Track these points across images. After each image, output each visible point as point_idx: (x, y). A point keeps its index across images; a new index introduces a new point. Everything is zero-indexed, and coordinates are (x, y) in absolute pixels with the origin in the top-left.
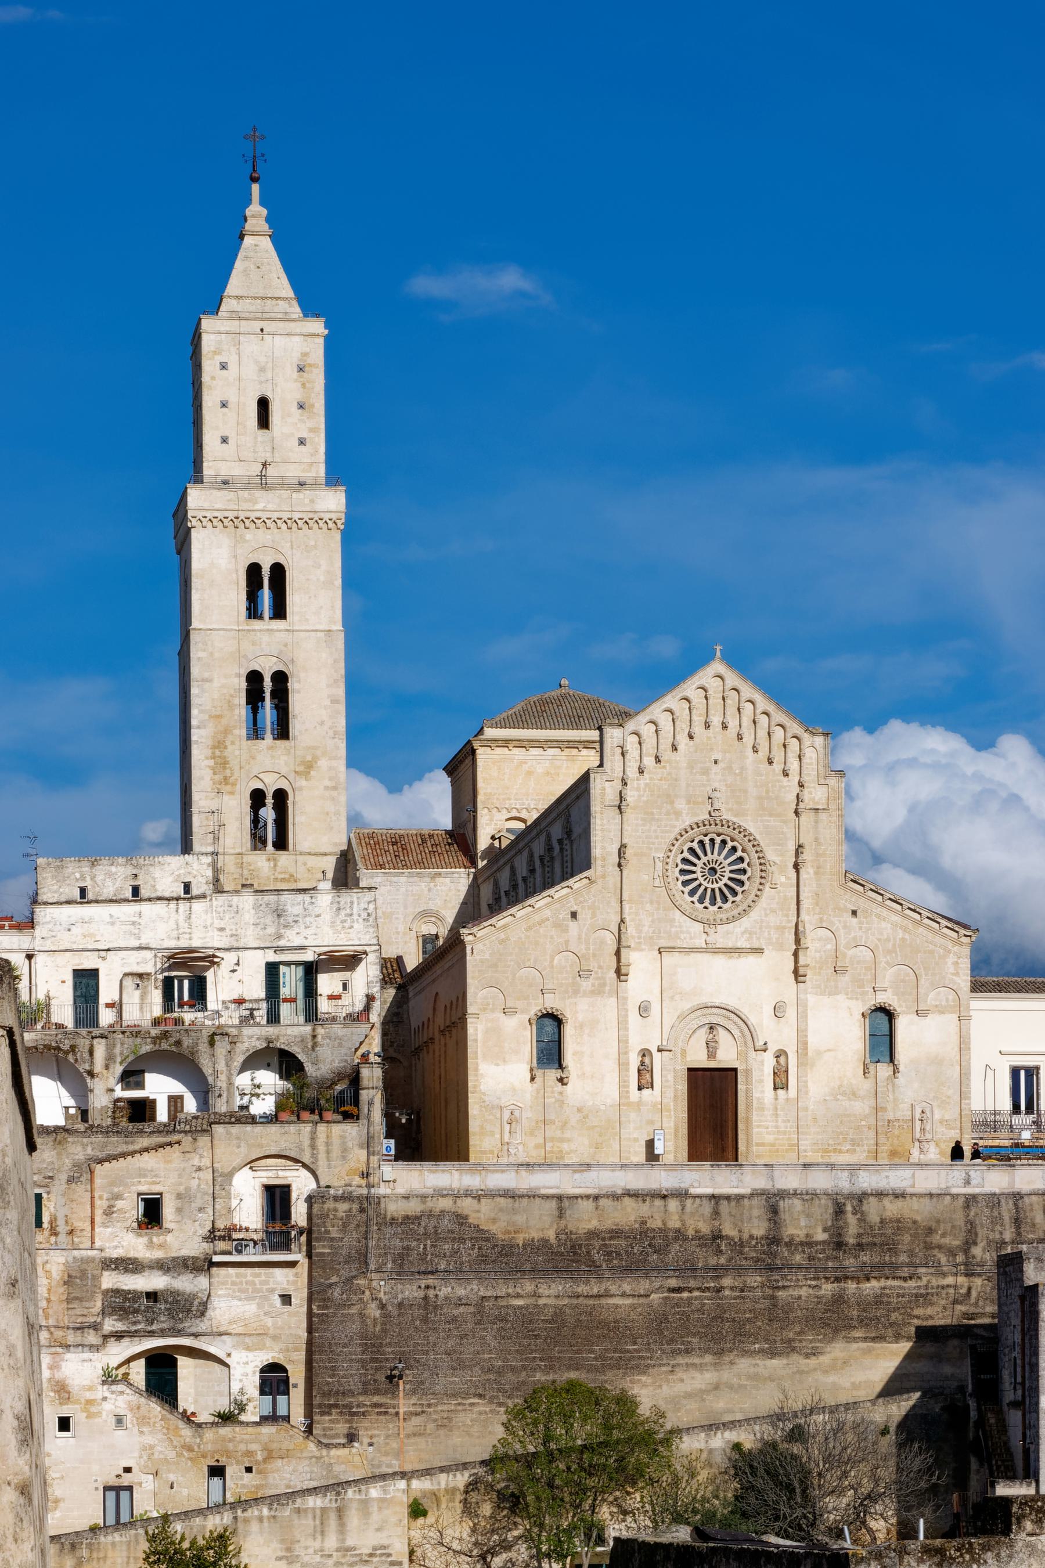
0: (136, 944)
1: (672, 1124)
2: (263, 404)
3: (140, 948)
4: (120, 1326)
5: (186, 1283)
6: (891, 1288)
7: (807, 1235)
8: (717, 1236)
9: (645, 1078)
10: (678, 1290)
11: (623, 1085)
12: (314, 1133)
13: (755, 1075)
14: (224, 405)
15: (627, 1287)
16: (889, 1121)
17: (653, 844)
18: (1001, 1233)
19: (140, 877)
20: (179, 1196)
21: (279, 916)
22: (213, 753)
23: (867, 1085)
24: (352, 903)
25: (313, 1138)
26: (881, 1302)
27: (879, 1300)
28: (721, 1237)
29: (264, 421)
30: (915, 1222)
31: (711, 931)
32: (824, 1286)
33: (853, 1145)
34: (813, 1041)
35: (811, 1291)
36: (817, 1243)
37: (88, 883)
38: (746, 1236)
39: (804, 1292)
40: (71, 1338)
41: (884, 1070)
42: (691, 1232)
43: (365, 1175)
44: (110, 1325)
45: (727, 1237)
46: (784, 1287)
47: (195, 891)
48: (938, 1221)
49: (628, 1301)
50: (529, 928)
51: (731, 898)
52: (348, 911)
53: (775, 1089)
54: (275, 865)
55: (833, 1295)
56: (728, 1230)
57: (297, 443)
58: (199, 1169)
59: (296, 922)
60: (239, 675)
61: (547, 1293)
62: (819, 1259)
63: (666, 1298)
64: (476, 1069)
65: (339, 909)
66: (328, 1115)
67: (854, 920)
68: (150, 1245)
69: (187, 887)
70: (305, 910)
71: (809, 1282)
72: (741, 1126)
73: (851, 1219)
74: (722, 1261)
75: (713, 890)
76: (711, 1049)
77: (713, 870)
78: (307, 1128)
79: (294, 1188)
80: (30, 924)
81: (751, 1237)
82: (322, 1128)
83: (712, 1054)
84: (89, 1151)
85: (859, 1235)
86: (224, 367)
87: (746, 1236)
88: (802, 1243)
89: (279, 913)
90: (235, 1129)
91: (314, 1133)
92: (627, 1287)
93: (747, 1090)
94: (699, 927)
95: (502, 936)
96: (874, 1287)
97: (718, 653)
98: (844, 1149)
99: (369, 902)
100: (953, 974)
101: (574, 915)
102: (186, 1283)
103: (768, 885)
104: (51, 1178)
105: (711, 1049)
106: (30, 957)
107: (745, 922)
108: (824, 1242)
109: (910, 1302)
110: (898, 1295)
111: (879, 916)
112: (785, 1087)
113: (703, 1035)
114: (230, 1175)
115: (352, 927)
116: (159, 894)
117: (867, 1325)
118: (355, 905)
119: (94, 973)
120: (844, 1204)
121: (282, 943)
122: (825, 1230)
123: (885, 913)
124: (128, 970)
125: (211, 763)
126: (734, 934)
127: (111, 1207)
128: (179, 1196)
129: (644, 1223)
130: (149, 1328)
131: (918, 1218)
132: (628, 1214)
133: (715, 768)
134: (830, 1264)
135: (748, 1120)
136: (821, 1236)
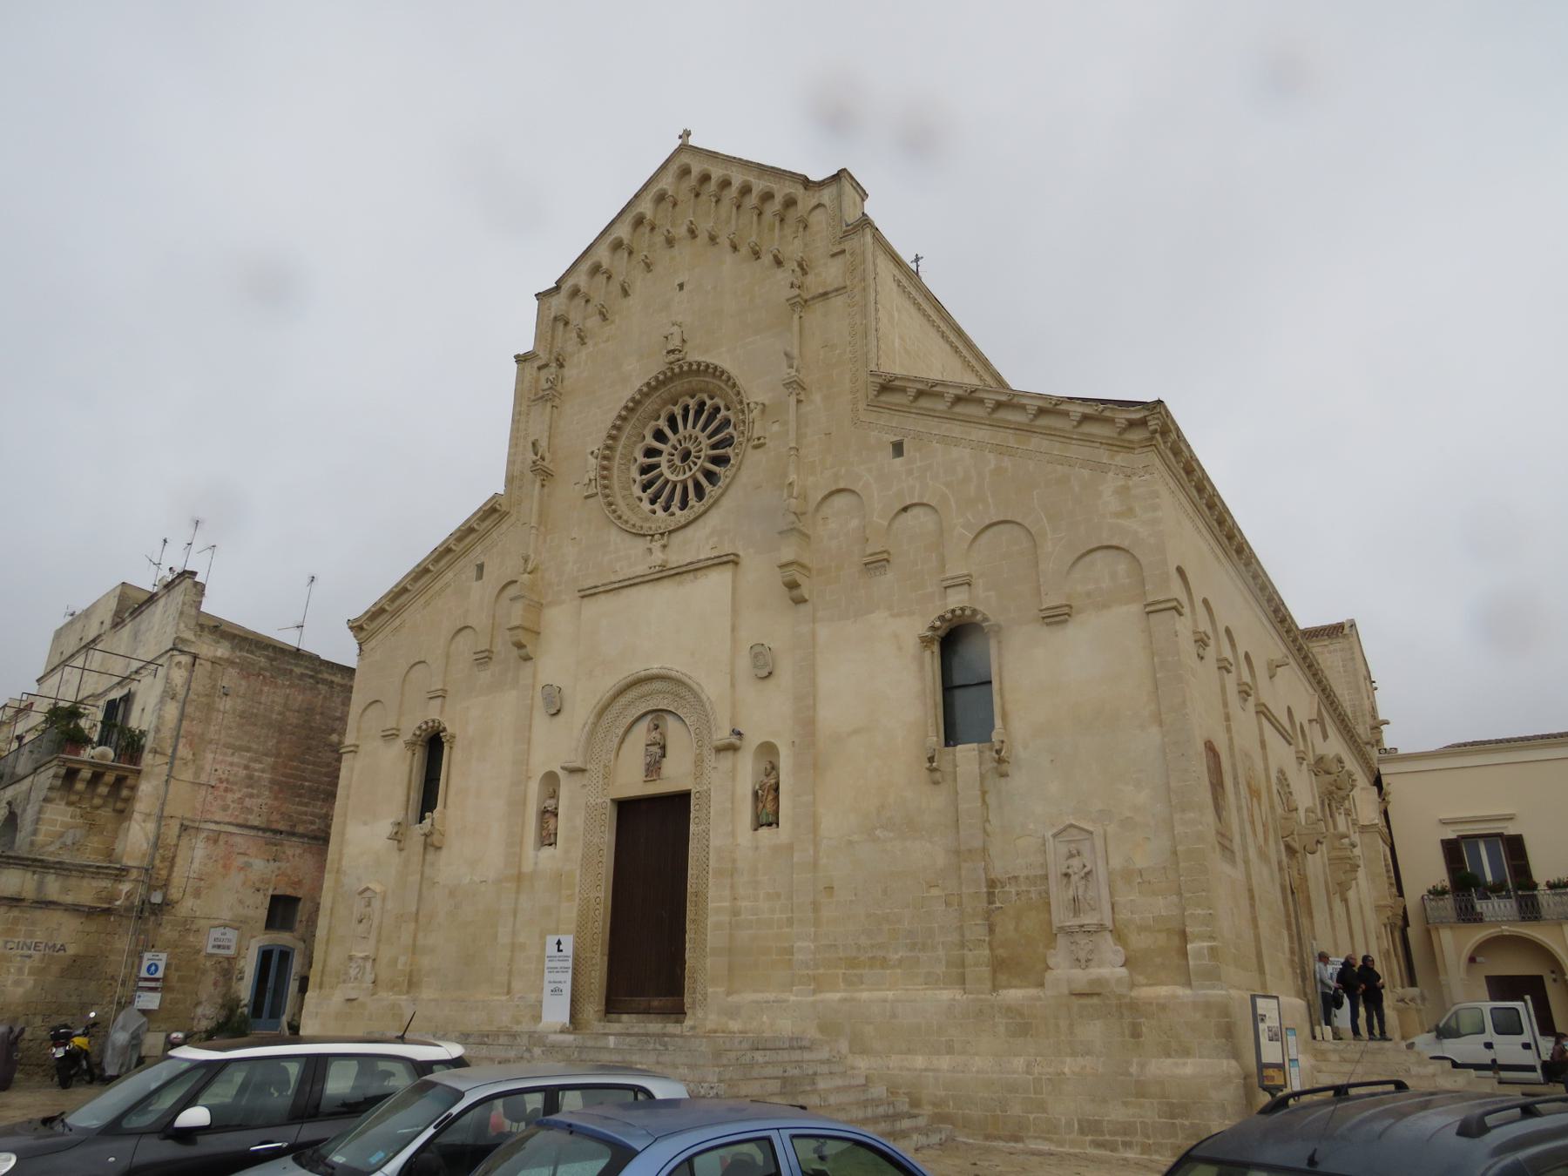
1: (574, 914)
11: (514, 843)
13: (717, 801)
16: (992, 884)
31: (656, 545)
33: (913, 947)
34: (830, 716)
50: (427, 604)
64: (343, 834)
75: (662, 475)
77: (686, 456)
83: (653, 769)
94: (642, 544)
95: (398, 622)
100: (1118, 515)
111: (945, 439)
112: (774, 822)
113: (641, 733)
123: (956, 430)
126: (697, 542)
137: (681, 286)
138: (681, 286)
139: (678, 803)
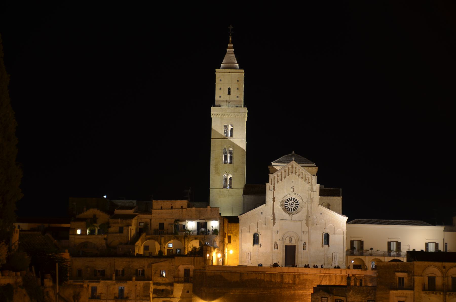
0: (172, 218)
2: (229, 89)
3: (172, 219)
4: (156, 296)
5: (169, 288)
6: (304, 293)
7: (288, 282)
8: (271, 281)
9: (276, 246)
10: (263, 292)
12: (194, 259)
14: (220, 89)
15: (253, 291)
18: (326, 283)
19: (173, 205)
20: (168, 271)
21: (200, 213)
22: (215, 167)
23: (323, 249)
24: (214, 211)
25: (194, 260)
26: (302, 296)
27: (302, 295)
28: (271, 281)
29: (229, 93)
30: (310, 280)
32: (291, 292)
35: (289, 293)
36: (290, 283)
37: (162, 206)
38: (276, 281)
39: (287, 293)
40: (144, 298)
41: (327, 246)
42: (266, 280)
43: (203, 267)
44: (154, 296)
45: (273, 282)
46: (283, 292)
47: (183, 207)
48: (314, 280)
49: (253, 294)
51: (295, 210)
52: (213, 212)
53: (304, 249)
54: (228, 192)
55: (293, 294)
56: (273, 280)
57: (236, 97)
58: (172, 266)
59: (203, 214)
61: (237, 292)
62: (290, 287)
63: (260, 293)
65: (212, 212)
66: (197, 255)
68: (163, 280)
69: (182, 207)
70: (205, 212)
71: (288, 291)
72: (296, 257)
73: (297, 279)
74: (272, 286)
76: (291, 241)
78: (193, 258)
79: (190, 270)
80: (150, 213)
81: (277, 282)
82: (196, 258)
84: (152, 262)
85: (298, 282)
86: (221, 80)
87: (276, 281)
88: (287, 283)
89: (200, 212)
90: (179, 258)
91: (194, 259)
92: (253, 291)
93: (297, 250)
96: (301, 293)
97: (293, 159)
98: (318, 262)
99: (218, 210)
101: (262, 213)
102: (169, 288)
104: (144, 267)
105: (291, 241)
107: (298, 215)
108: (291, 283)
109: (308, 296)
110: (306, 294)
114: (178, 267)
115: (214, 215)
116: (176, 208)
117: (299, 300)
118: (215, 211)
119: (163, 224)
120: (296, 276)
121: (200, 218)
122: (292, 281)
124: (169, 223)
125: (215, 169)
126: (295, 217)
127: (155, 272)
128: (168, 271)
129: (257, 278)
130: (162, 297)
131: (310, 279)
132: (253, 276)
133: (292, 183)
134: (293, 288)
135: (297, 256)
136: (291, 282)
137: (292, 182)
139: (294, 246)
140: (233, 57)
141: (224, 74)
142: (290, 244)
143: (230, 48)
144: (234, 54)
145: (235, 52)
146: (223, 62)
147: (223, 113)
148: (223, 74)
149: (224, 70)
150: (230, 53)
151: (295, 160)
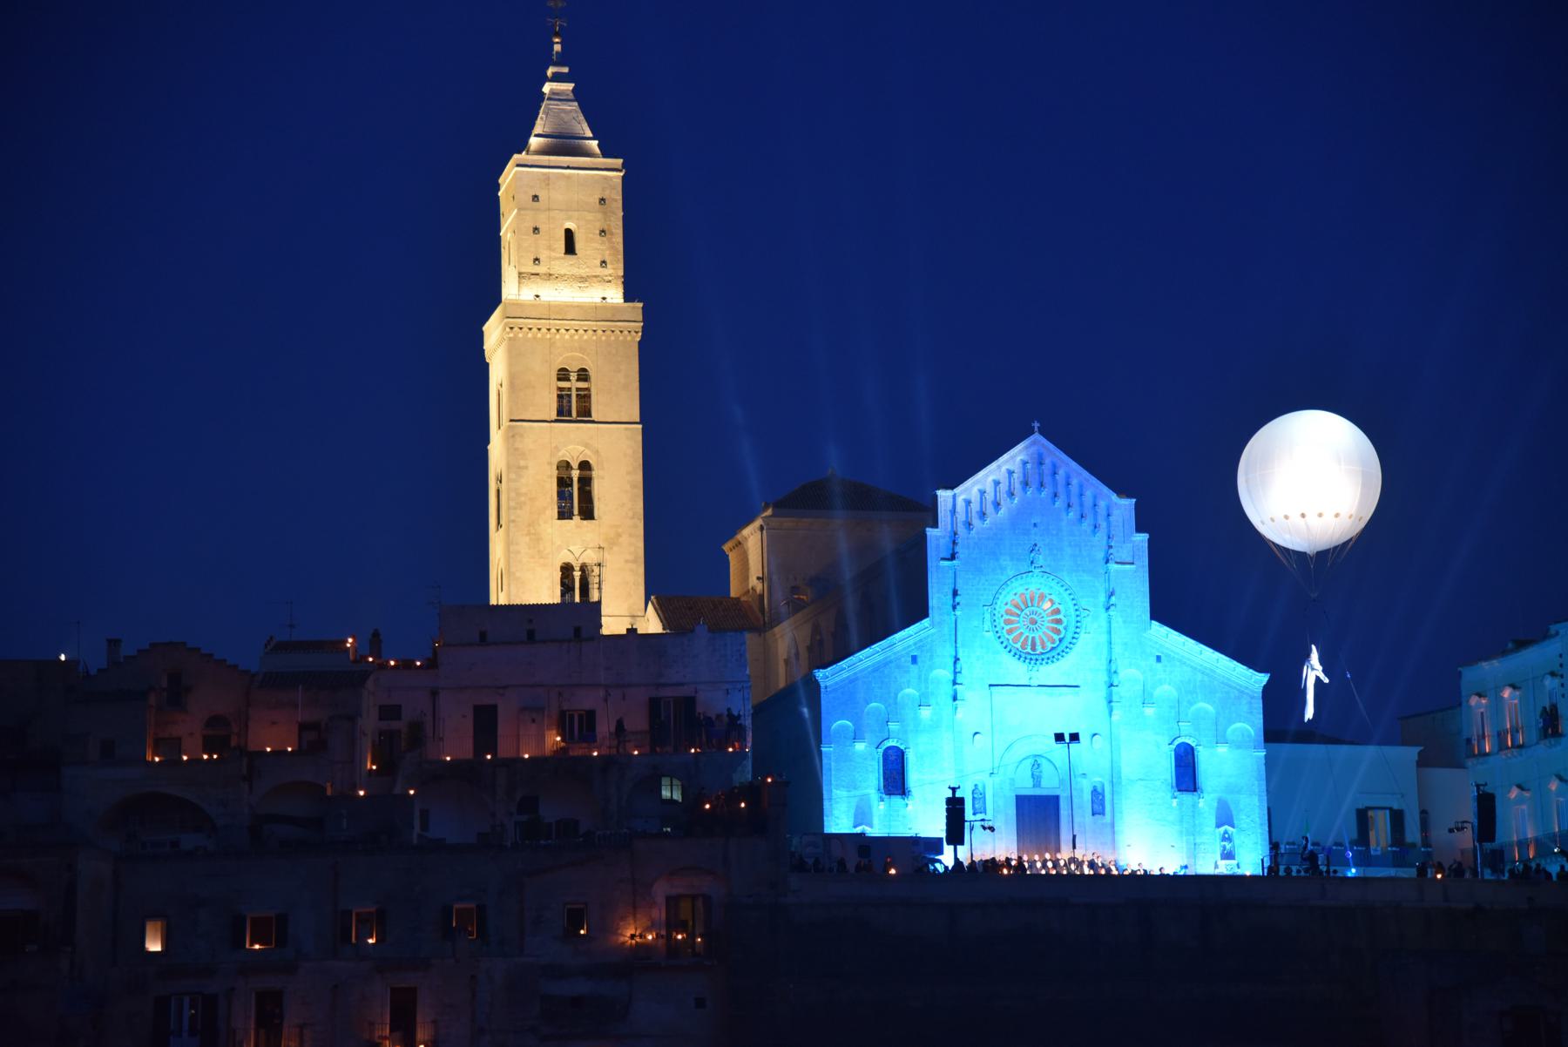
2: (569, 235)
17: (982, 595)
29: (570, 248)
53: (1093, 814)
60: (550, 464)
67: (1159, 665)
77: (1034, 622)
97: (1036, 429)
103: (1083, 631)
106: (434, 694)
112: (1103, 813)
138: (1035, 525)
140: (575, 115)
141: (549, 173)
142: (1038, 792)
143: (557, 78)
144: (576, 104)
145: (578, 95)
146: (538, 129)
147: (551, 321)
148: (544, 174)
149: (547, 157)
150: (555, 96)
151: (1042, 432)
